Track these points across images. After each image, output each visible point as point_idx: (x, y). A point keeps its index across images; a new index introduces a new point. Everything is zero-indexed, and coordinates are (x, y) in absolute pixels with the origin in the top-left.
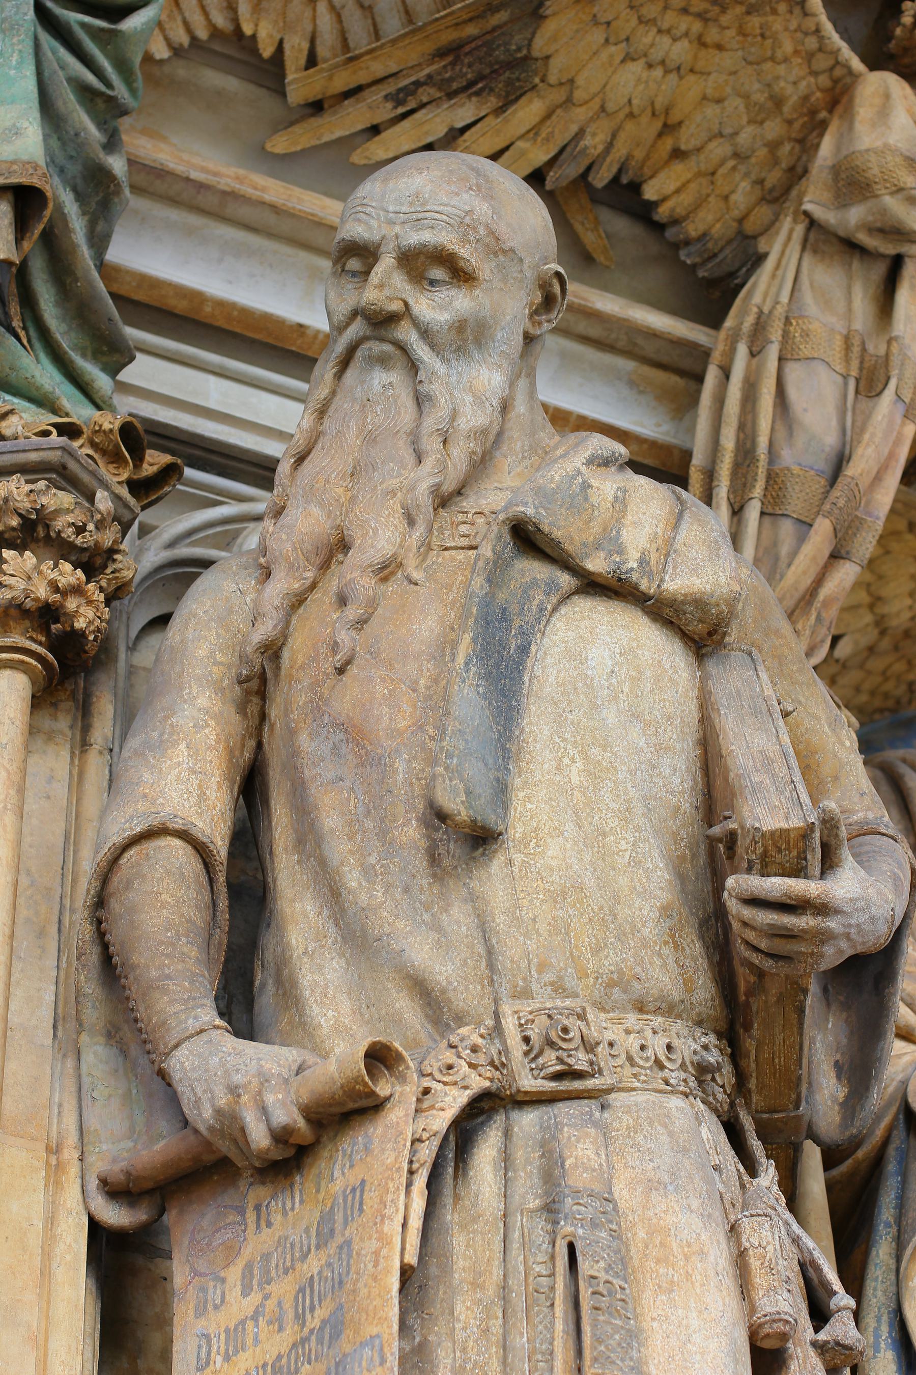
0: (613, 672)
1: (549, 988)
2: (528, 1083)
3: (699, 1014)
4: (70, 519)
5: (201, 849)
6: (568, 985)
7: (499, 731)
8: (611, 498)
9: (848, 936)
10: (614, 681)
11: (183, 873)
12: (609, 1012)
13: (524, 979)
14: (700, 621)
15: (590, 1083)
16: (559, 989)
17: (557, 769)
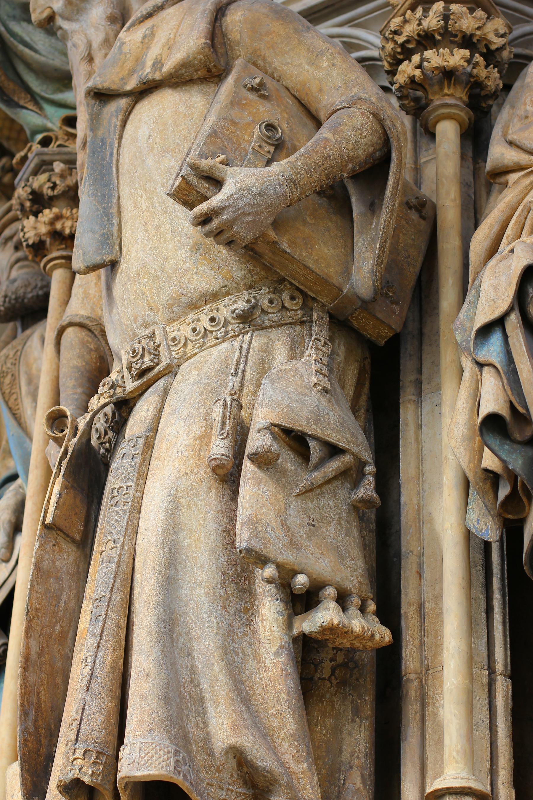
0: (149, 136)
1: (143, 328)
2: (130, 385)
3: (245, 284)
4: (47, 186)
5: (81, 325)
6: (149, 321)
7: (104, 208)
8: (140, 39)
9: (244, 214)
10: (151, 141)
11: (72, 344)
12: (178, 320)
13: (132, 330)
14: (196, 71)
15: (156, 370)
16: (146, 325)
17: (135, 207)
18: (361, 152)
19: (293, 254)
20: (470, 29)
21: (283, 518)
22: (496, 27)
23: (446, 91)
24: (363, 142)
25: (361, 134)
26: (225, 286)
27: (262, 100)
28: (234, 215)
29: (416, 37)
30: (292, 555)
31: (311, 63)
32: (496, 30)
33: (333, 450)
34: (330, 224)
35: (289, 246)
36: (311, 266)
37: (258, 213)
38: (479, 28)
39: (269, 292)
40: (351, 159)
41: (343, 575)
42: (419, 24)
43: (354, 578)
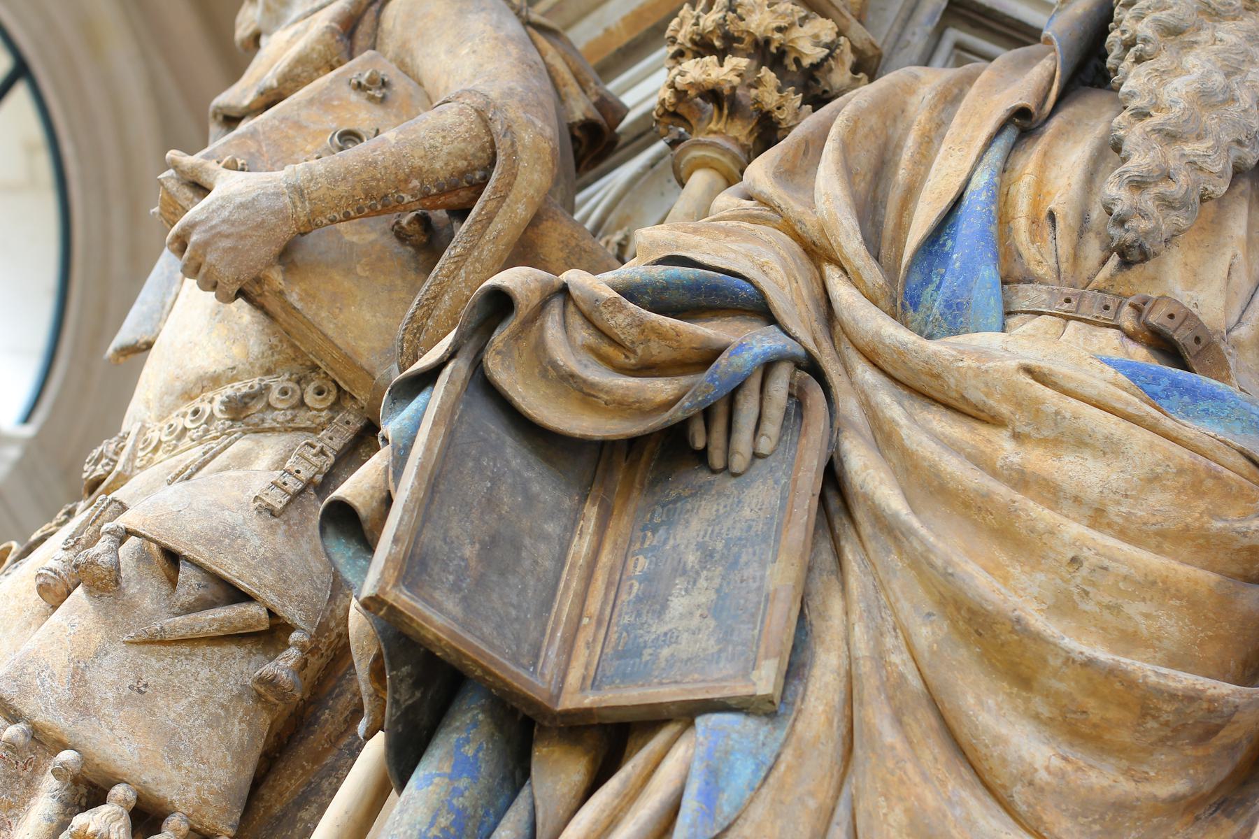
3: (261, 367)
9: (221, 235)
18: (438, 165)
19: (304, 312)
20: (762, 29)
21: (82, 665)
22: (816, 31)
23: (712, 126)
24: (446, 149)
25: (444, 137)
26: (234, 368)
27: (369, 105)
28: (207, 236)
29: (689, 45)
30: (66, 719)
31: (451, 51)
32: (816, 36)
33: (237, 595)
34: (399, 282)
35: (301, 299)
36: (330, 333)
37: (242, 237)
38: (780, 29)
39: (289, 380)
40: (416, 172)
41: (164, 777)
42: (697, 24)
43: (192, 789)
